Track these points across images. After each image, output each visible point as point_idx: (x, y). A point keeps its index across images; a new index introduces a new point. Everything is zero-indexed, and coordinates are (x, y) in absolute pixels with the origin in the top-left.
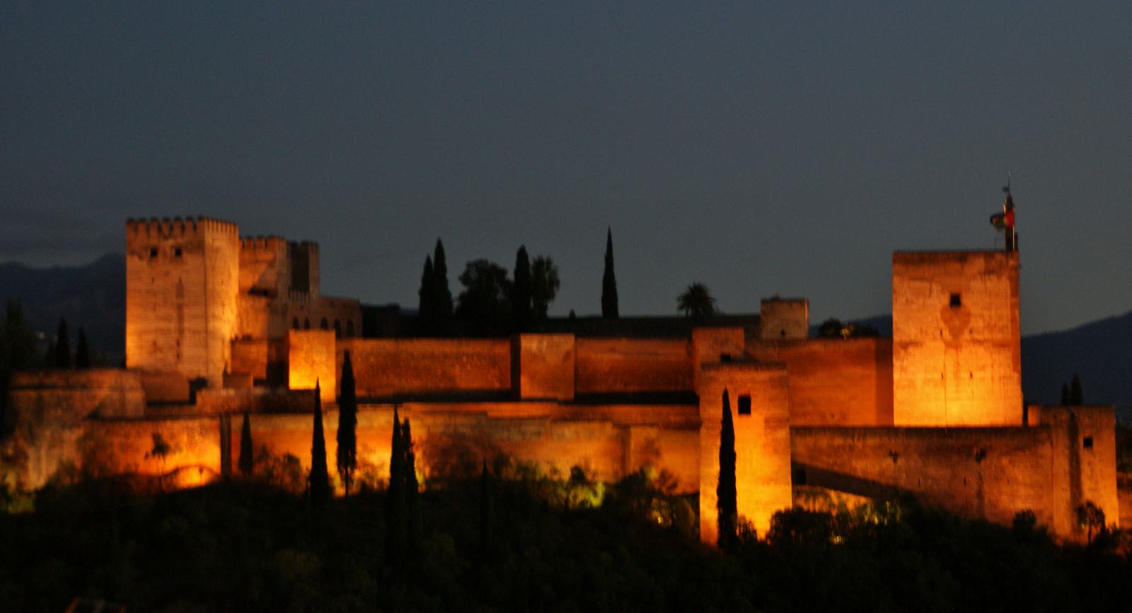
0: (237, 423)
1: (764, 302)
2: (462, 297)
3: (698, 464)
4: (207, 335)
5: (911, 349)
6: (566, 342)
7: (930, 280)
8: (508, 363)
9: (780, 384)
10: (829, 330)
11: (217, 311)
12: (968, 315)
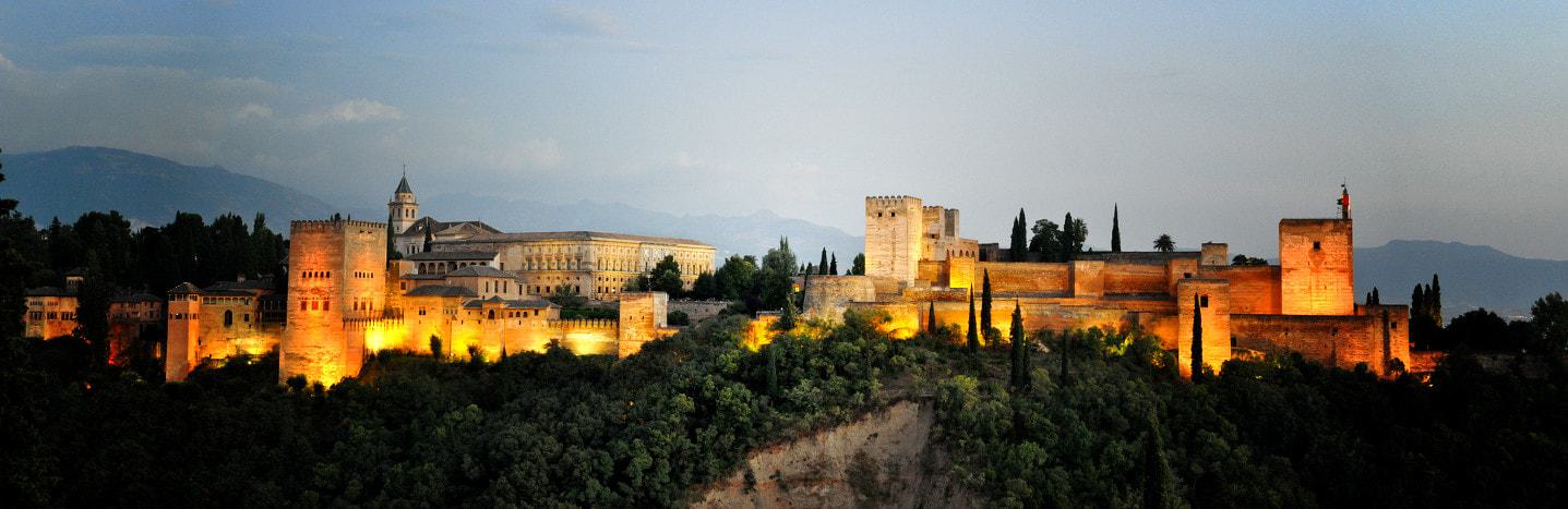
0: (927, 306)
1: (1203, 245)
2: (1034, 241)
3: (1177, 333)
4: (907, 258)
5: (1292, 273)
6: (1100, 265)
7: (1303, 234)
8: (1067, 276)
9: (1225, 290)
10: (1240, 260)
11: (911, 245)
12: (1324, 254)
